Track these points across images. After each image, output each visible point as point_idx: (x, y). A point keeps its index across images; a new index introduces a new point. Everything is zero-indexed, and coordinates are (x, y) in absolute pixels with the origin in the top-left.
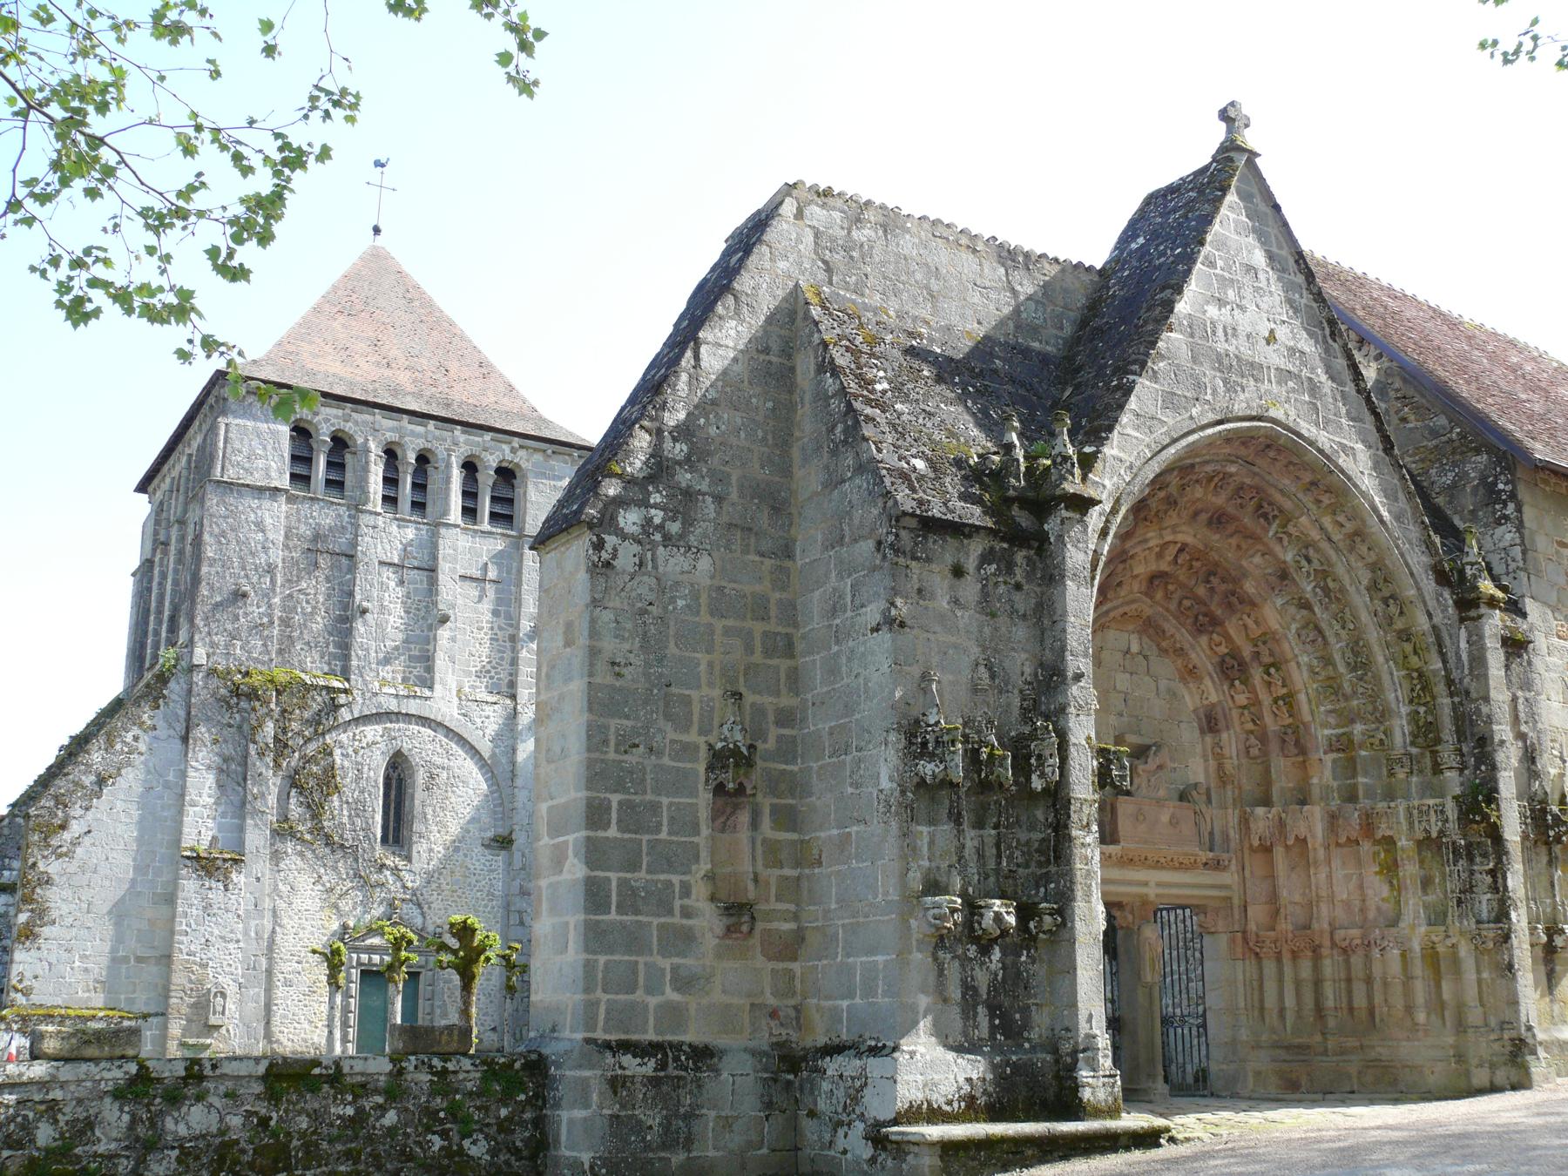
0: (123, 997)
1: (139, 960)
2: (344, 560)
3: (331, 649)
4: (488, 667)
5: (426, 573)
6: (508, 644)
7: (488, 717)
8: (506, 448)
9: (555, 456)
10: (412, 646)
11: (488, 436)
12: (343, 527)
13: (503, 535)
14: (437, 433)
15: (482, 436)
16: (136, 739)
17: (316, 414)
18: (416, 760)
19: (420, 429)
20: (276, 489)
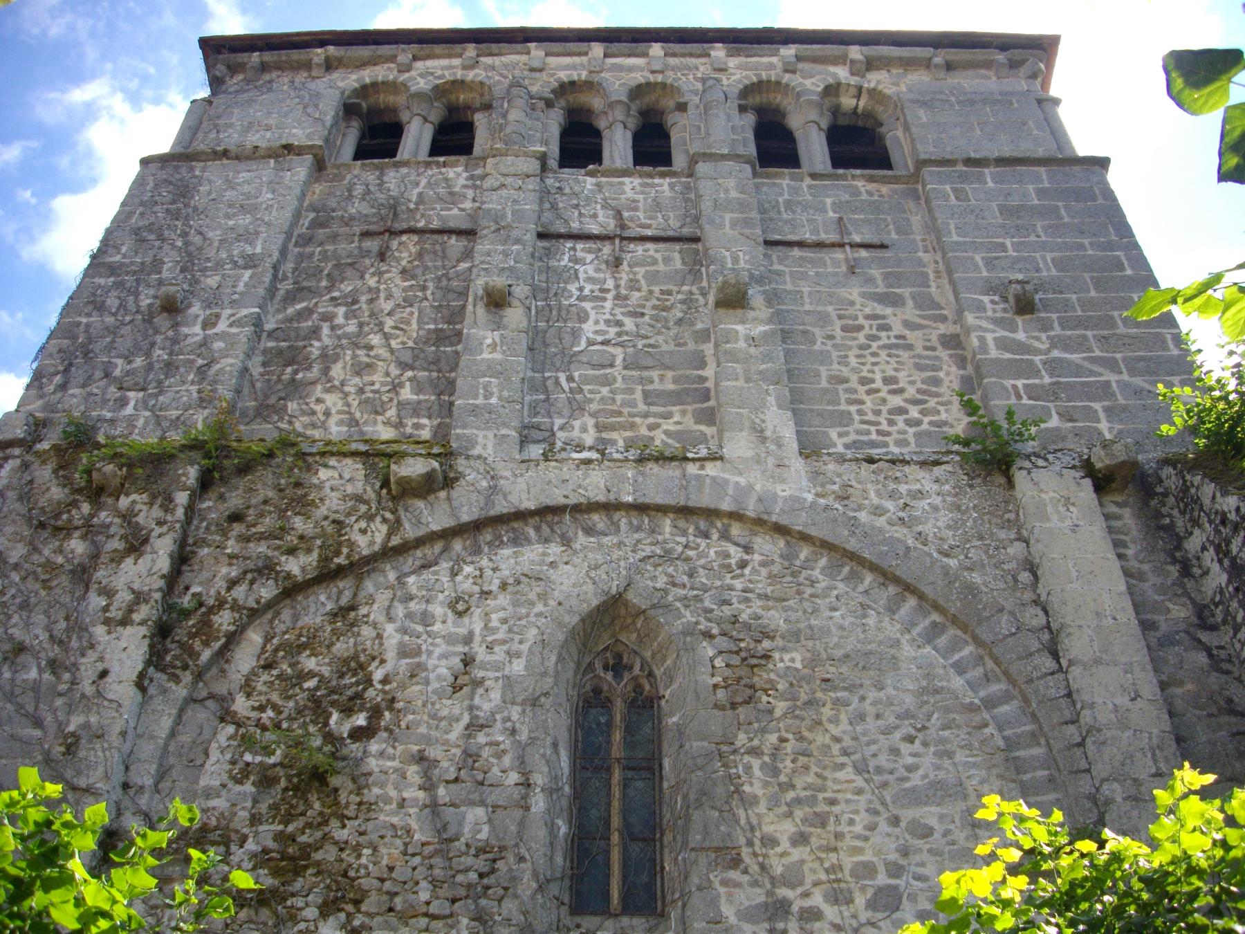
2: (455, 244)
3: (407, 393)
4: (896, 401)
5: (677, 247)
6: (944, 354)
7: (919, 495)
8: (842, 73)
10: (655, 374)
11: (789, 51)
12: (452, 194)
13: (871, 179)
14: (673, 61)
20: (288, 148)
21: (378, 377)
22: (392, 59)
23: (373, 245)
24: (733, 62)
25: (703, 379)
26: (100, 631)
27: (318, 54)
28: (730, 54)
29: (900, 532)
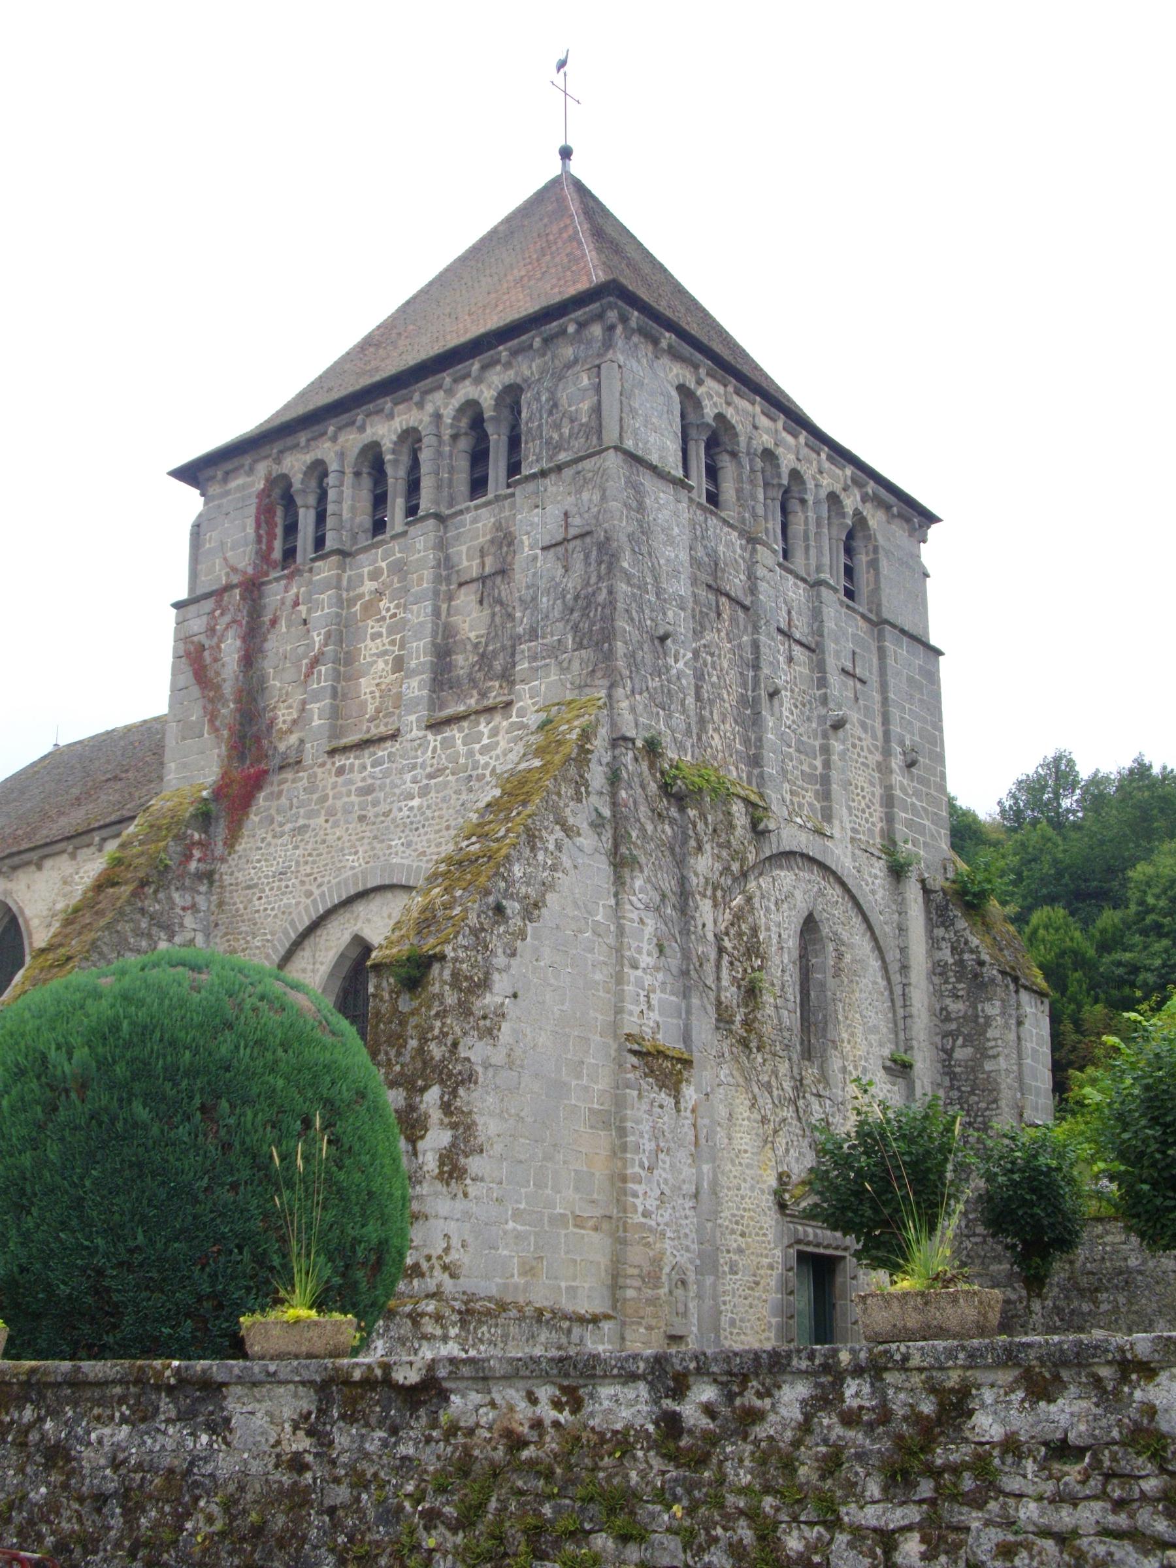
0: (563, 1284)
1: (579, 1222)
9: (897, 521)
15: (842, 468)
16: (559, 847)
17: (700, 382)
18: (825, 930)
19: (790, 439)
21: (727, 726)
22: (696, 367)
23: (712, 597)
24: (827, 465)
25: (816, 768)
26: (698, 897)
27: (668, 338)
28: (829, 458)
29: (871, 897)
